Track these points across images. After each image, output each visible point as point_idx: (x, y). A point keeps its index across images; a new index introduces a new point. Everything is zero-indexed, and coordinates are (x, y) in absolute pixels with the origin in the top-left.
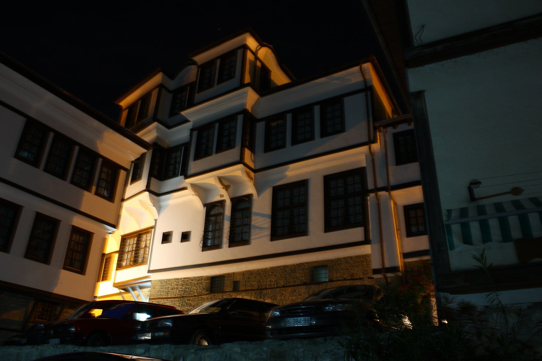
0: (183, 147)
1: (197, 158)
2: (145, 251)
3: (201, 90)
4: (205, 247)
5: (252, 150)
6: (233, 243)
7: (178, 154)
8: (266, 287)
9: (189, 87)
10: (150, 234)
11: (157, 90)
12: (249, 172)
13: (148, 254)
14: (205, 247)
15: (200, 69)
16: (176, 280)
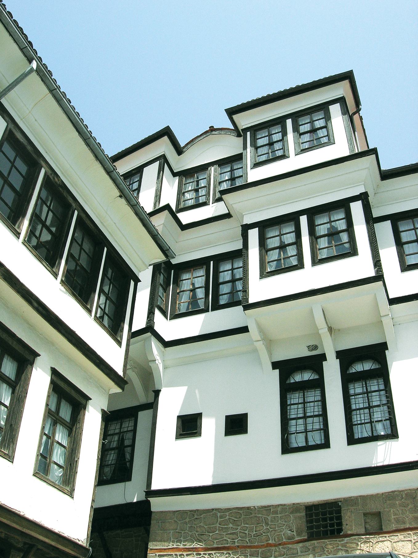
0: (212, 262)
16: (214, 511)
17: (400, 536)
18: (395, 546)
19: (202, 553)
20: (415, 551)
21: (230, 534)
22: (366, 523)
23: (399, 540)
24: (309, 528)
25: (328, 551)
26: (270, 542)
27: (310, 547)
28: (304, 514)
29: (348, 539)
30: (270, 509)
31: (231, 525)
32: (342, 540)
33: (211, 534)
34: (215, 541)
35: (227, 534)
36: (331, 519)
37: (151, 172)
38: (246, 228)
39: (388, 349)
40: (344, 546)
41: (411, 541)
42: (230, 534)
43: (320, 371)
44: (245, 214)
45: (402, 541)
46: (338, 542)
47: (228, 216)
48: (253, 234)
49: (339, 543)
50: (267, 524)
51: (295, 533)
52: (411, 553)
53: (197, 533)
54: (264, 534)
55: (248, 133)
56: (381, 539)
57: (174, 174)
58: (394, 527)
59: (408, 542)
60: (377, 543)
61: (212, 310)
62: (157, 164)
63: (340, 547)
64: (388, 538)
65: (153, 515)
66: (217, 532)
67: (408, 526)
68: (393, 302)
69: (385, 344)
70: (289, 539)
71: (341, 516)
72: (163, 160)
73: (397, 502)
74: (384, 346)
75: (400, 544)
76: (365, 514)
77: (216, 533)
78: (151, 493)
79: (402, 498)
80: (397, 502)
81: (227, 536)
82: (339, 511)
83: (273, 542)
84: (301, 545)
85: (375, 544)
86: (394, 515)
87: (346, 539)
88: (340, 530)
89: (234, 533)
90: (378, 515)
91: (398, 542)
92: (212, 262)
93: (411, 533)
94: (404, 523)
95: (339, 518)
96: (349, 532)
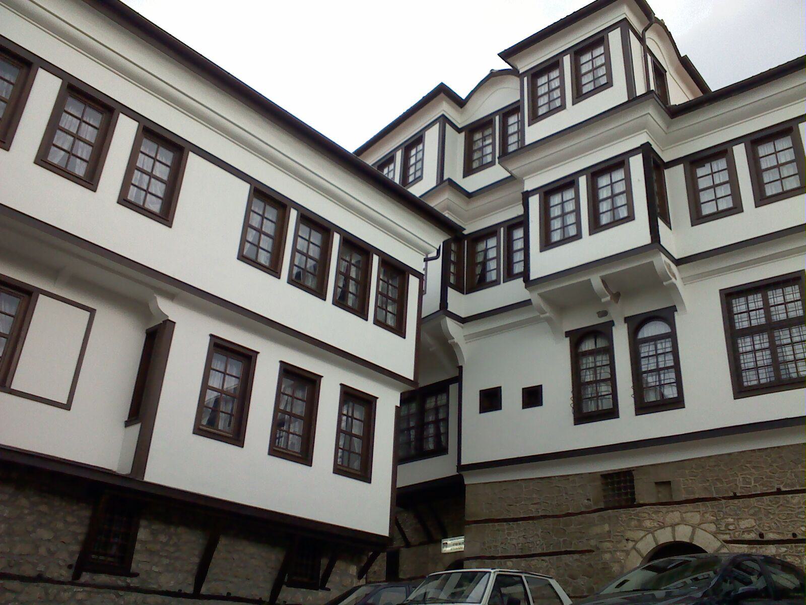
0: (502, 229)
1: (547, 244)
2: (437, 429)
3: (535, 118)
4: (581, 417)
5: (668, 223)
6: (643, 407)
7: (492, 242)
8: (735, 494)
9: (497, 118)
10: (444, 397)
11: (436, 128)
12: (669, 264)
13: (447, 433)
14: (581, 417)
15: (525, 79)
16: (519, 482)
17: (689, 507)
18: (684, 516)
19: (511, 523)
20: (703, 522)
21: (535, 504)
22: (659, 492)
23: (687, 511)
24: (605, 497)
25: (622, 520)
26: (570, 511)
27: (606, 517)
28: (598, 483)
29: (640, 508)
30: (569, 479)
31: (534, 496)
32: (636, 510)
33: (518, 505)
34: (521, 512)
35: (532, 504)
36: (625, 488)
37: (432, 137)
38: (526, 195)
39: (676, 311)
40: (636, 515)
41: (699, 511)
42: (535, 504)
43: (610, 338)
44: (527, 179)
45: (692, 512)
46: (631, 511)
47: (511, 179)
48: (534, 202)
49: (632, 512)
50: (566, 493)
51: (591, 503)
52: (700, 524)
53: (506, 504)
54: (564, 504)
55: (525, 79)
56: (671, 509)
57: (459, 130)
58: (684, 497)
59: (696, 513)
60: (667, 514)
61: (504, 282)
62: (436, 128)
63: (633, 517)
64: (677, 509)
65: (467, 488)
66: (523, 503)
67: (697, 496)
68: (678, 262)
69: (675, 306)
70: (586, 507)
71: (634, 485)
72: (444, 120)
73: (687, 471)
74: (673, 309)
75: (689, 514)
76: (656, 483)
77: (523, 503)
78: (461, 468)
79: (692, 468)
80: (687, 471)
81: (532, 505)
82: (632, 481)
83: (573, 511)
84: (597, 514)
85: (666, 513)
86: (684, 486)
87: (639, 509)
88: (634, 499)
89: (538, 503)
90: (668, 483)
91: (687, 512)
92: (502, 229)
93: (699, 503)
94: (694, 493)
95: (633, 487)
96: (641, 502)
